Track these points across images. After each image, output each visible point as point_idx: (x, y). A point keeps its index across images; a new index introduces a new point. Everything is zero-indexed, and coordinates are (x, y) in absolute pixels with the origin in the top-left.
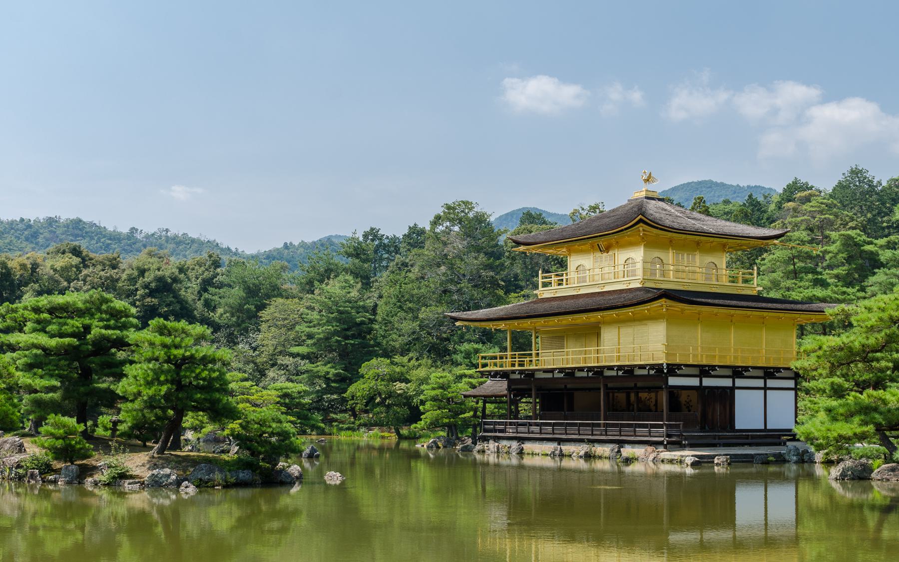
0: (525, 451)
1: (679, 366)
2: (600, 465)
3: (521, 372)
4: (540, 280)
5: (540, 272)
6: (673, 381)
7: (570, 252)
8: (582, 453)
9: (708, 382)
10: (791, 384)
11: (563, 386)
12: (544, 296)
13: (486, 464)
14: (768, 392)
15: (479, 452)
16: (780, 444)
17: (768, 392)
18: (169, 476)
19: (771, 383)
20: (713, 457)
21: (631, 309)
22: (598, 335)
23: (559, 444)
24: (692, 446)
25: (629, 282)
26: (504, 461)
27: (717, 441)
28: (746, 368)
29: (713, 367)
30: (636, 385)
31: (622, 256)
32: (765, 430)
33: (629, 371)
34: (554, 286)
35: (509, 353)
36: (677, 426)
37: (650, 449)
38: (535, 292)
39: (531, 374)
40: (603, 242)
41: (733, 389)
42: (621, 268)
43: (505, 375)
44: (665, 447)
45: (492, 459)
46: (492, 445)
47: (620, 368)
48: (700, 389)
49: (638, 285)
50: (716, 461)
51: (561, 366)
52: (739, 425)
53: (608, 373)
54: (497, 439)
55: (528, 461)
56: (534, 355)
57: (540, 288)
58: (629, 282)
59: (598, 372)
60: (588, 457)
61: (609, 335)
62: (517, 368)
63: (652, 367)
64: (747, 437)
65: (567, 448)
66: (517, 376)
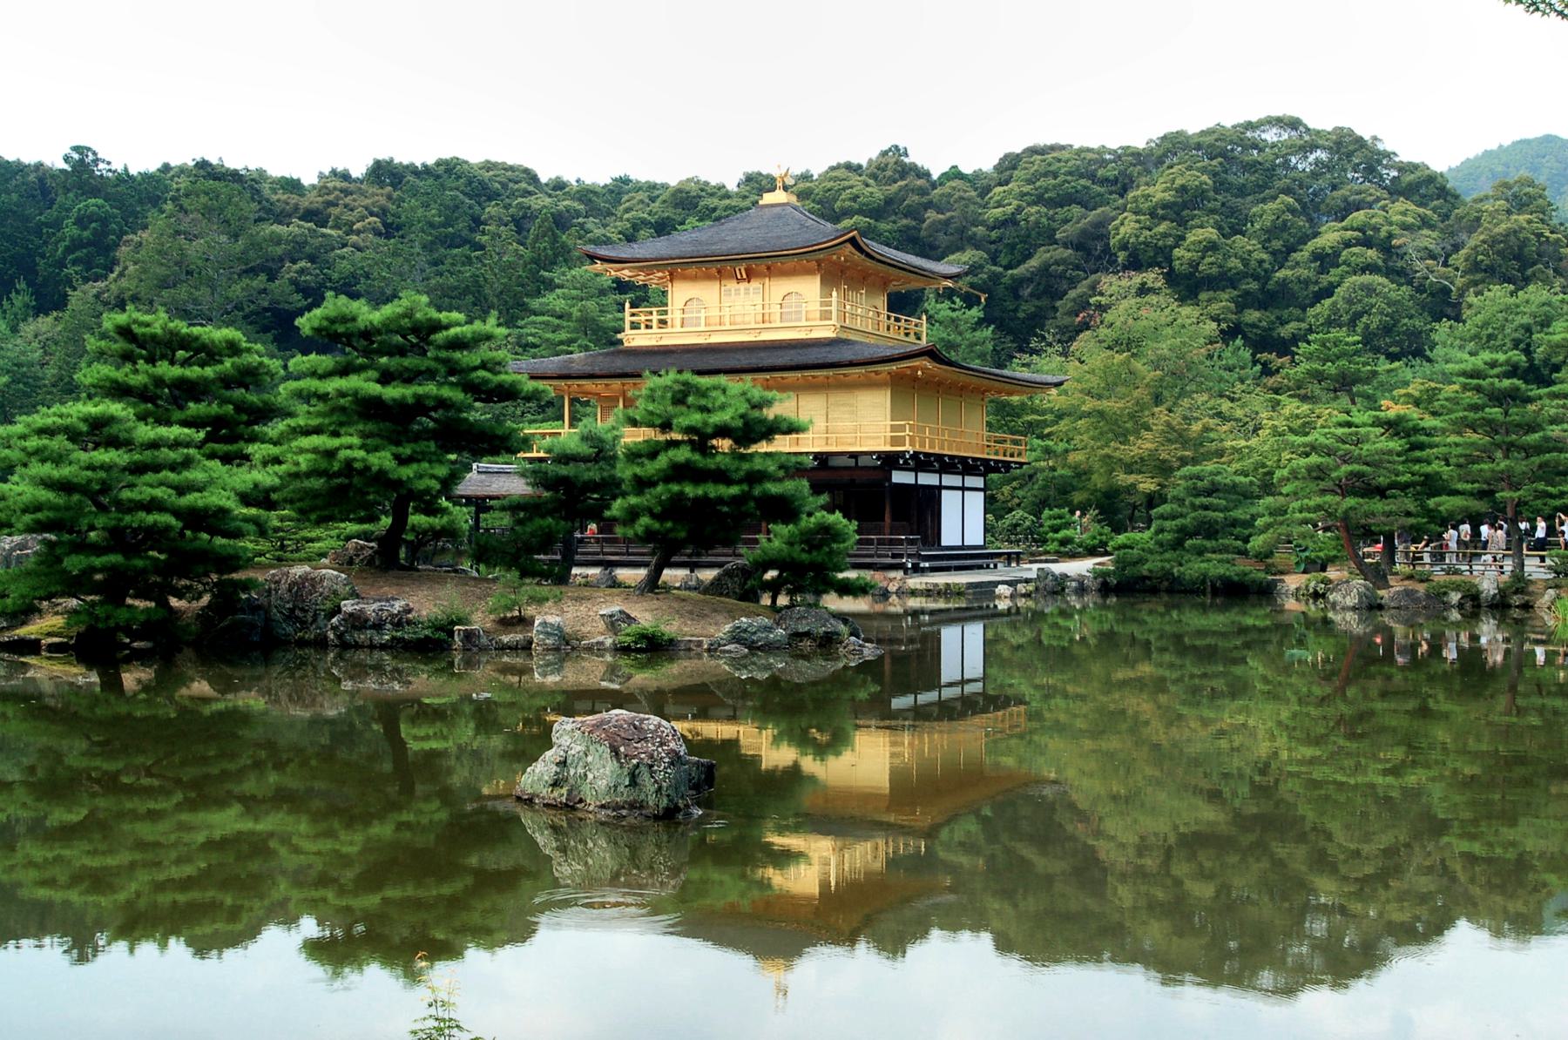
4: (628, 319)
5: (627, 305)
6: (899, 477)
7: (672, 278)
10: (978, 482)
12: (634, 344)
18: (769, 629)
19: (972, 481)
25: (811, 328)
29: (940, 457)
31: (779, 288)
32: (963, 547)
34: (655, 330)
36: (912, 542)
41: (940, 488)
47: (817, 456)
48: (916, 487)
49: (829, 334)
52: (944, 543)
57: (628, 331)
58: (811, 328)
63: (880, 455)
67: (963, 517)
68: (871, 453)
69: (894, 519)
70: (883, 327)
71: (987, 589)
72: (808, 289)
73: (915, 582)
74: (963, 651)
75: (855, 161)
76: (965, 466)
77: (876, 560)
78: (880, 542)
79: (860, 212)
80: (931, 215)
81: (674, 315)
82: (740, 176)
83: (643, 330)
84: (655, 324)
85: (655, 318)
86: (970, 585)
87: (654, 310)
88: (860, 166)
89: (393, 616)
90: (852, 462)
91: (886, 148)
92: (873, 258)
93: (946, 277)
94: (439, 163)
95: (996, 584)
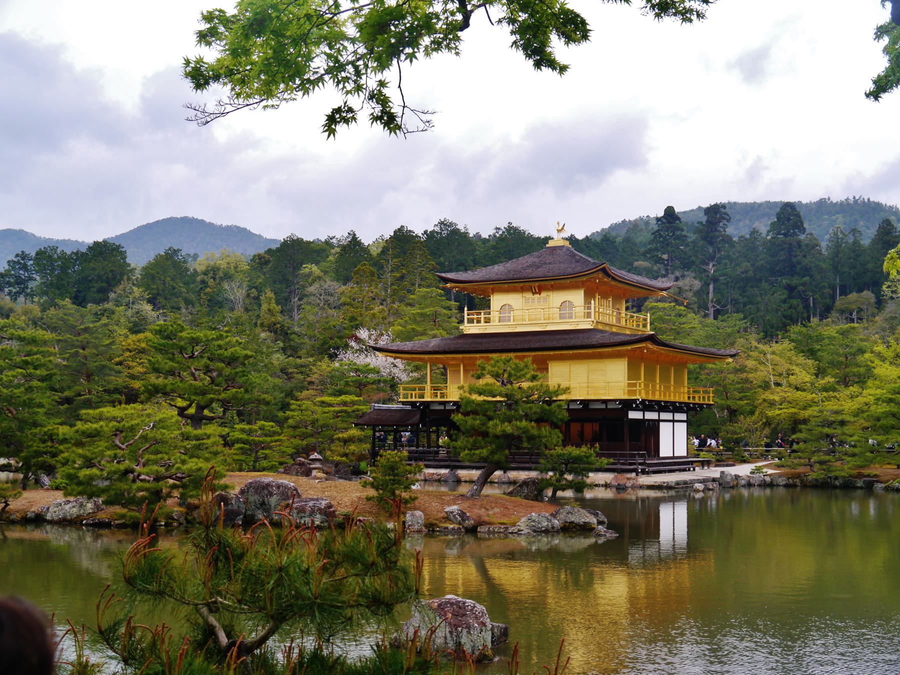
0: (463, 479)
4: (466, 317)
6: (633, 415)
7: (494, 291)
9: (651, 416)
10: (683, 417)
16: (689, 470)
23: (505, 472)
32: (673, 457)
34: (483, 323)
37: (619, 476)
43: (427, 404)
44: (637, 475)
47: (583, 402)
48: (643, 421)
52: (661, 455)
58: (578, 323)
63: (622, 401)
67: (674, 439)
68: (615, 400)
70: (623, 323)
71: (687, 485)
72: (577, 297)
73: (645, 480)
74: (674, 522)
76: (675, 407)
78: (622, 455)
81: (494, 315)
83: (475, 324)
84: (482, 320)
86: (678, 483)
89: (320, 509)
90: (603, 406)
92: (616, 280)
93: (662, 290)
95: (693, 482)
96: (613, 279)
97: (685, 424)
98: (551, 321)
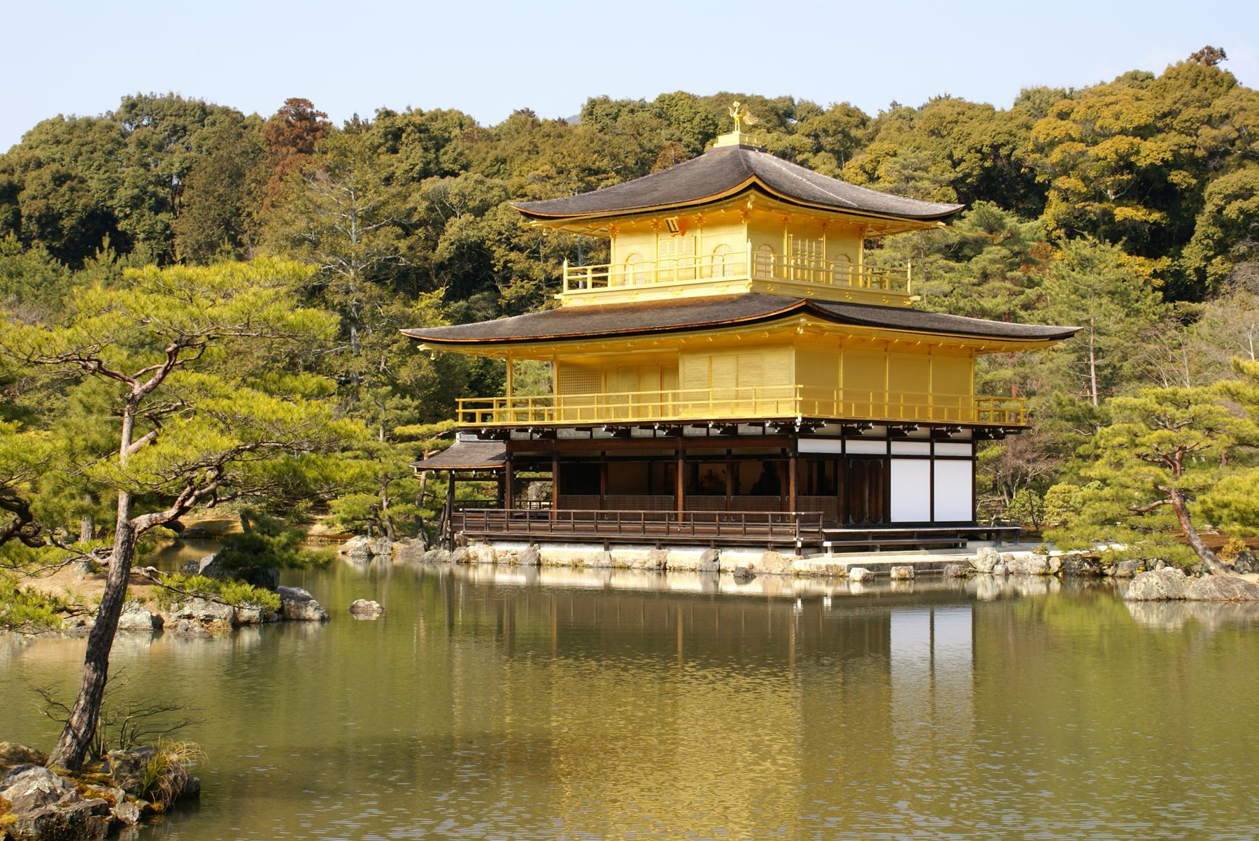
1: (817, 422)
2: (676, 583)
3: (537, 429)
4: (566, 278)
5: (566, 263)
6: (805, 446)
8: (653, 563)
9: (854, 447)
10: (966, 449)
11: (599, 453)
13: (470, 585)
14: (936, 462)
15: (458, 562)
16: (956, 546)
17: (936, 462)
19: (941, 448)
20: (888, 566)
21: (745, 330)
22: (674, 370)
23: (607, 549)
24: (837, 549)
26: (504, 578)
27: (870, 542)
28: (910, 426)
30: (729, 451)
32: (932, 523)
33: (729, 428)
34: (590, 289)
35: (508, 398)
38: (556, 296)
39: (549, 433)
40: (674, 219)
41: (888, 458)
42: (706, 262)
43: (502, 434)
44: (799, 552)
45: (480, 575)
46: (479, 550)
47: (718, 423)
48: (843, 457)
49: (744, 289)
50: (894, 574)
51: (613, 420)
52: (895, 518)
53: (689, 431)
54: (490, 540)
55: (548, 578)
56: (555, 402)
59: (675, 429)
60: (662, 569)
61: (691, 367)
62: (531, 422)
63: (775, 422)
64: (911, 535)
65: (622, 554)
66: (522, 436)
69: (799, 493)
75: (1144, 68)
77: (770, 538)
79: (1123, 132)
80: (1205, 131)
82: (1016, 93)
84: (589, 284)
85: (590, 276)
87: (590, 268)
88: (1150, 77)
91: (1197, 51)
94: (661, 99)
95: (850, 567)
96: (782, 200)
97: (968, 465)
98: (698, 281)
